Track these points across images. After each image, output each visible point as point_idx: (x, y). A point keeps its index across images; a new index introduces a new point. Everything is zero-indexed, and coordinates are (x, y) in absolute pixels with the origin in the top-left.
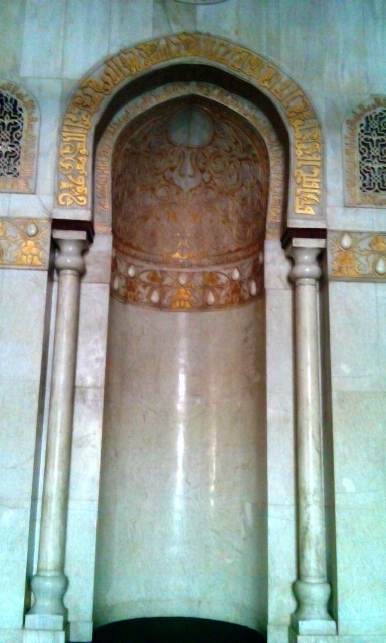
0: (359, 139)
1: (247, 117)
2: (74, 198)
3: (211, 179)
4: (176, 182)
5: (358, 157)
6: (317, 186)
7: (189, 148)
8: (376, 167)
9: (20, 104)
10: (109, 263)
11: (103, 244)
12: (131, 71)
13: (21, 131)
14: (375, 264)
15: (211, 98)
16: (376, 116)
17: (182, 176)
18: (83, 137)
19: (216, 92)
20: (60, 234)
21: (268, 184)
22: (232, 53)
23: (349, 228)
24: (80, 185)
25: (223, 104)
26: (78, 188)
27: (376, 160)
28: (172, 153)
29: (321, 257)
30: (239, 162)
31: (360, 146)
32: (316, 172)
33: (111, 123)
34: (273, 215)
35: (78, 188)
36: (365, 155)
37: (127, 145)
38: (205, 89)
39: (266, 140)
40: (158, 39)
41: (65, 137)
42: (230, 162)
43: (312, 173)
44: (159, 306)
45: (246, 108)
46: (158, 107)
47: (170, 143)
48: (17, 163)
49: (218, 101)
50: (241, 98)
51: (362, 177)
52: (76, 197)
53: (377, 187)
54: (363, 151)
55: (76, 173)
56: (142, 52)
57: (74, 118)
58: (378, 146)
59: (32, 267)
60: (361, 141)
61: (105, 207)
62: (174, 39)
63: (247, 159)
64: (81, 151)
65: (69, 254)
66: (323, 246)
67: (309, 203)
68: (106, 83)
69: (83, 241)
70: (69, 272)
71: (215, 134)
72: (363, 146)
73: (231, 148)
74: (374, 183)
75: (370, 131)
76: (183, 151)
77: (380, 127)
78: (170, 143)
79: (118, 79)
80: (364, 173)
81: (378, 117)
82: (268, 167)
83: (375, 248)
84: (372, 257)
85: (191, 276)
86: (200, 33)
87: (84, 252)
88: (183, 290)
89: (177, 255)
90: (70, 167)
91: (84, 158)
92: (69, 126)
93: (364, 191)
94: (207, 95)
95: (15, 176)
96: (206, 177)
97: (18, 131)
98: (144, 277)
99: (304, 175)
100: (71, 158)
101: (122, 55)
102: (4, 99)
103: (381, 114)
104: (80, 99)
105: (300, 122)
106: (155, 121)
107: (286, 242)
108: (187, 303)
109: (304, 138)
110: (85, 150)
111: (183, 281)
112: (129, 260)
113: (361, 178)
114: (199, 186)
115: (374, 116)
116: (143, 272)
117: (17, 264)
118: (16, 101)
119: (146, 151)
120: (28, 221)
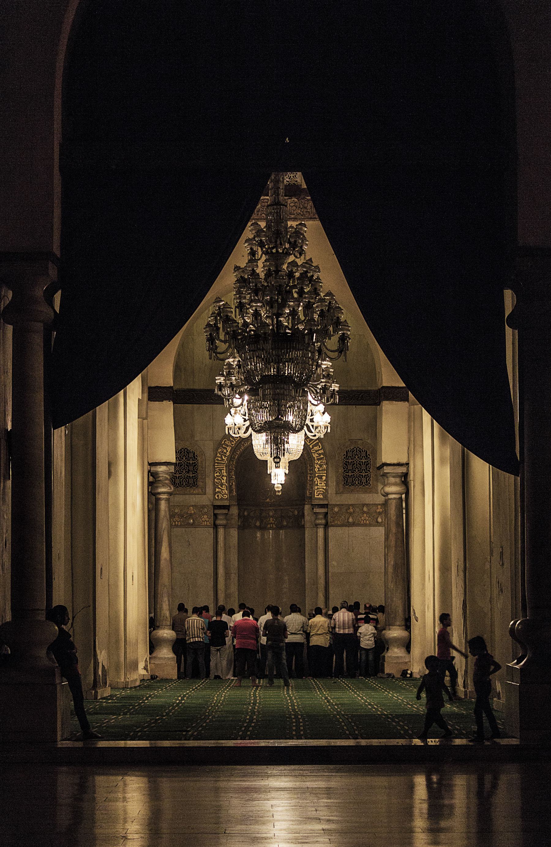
6: (324, 485)
11: (234, 511)
14: (348, 519)
20: (217, 511)
23: (338, 503)
32: (324, 478)
35: (223, 491)
52: (223, 495)
55: (222, 485)
59: (206, 526)
65: (221, 519)
67: (321, 492)
77: (352, 455)
83: (348, 511)
84: (347, 516)
85: (276, 511)
88: (271, 519)
92: (218, 463)
99: (319, 480)
103: (353, 449)
105: (317, 455)
108: (274, 525)
109: (319, 462)
110: (225, 474)
112: (245, 507)
116: (251, 512)
117: (199, 526)
120: (203, 507)
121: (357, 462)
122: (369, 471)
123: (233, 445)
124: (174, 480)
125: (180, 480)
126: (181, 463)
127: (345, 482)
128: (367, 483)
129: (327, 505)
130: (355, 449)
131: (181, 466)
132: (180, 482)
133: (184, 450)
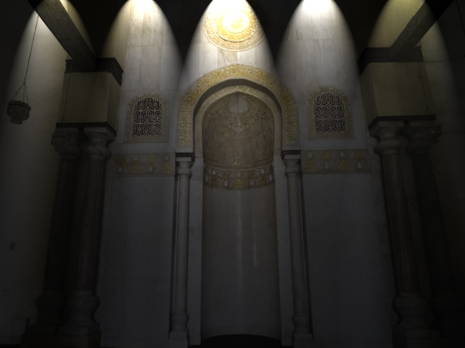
0: (314, 108)
1: (263, 100)
2: (185, 143)
3: (249, 127)
4: (233, 129)
5: (314, 116)
7: (238, 114)
8: (323, 120)
9: (160, 103)
10: (202, 170)
11: (199, 162)
12: (209, 84)
13: (161, 114)
15: (246, 92)
16: (322, 97)
17: (237, 127)
18: (188, 115)
19: (248, 89)
20: (179, 159)
21: (274, 130)
22: (254, 72)
24: (188, 137)
25: (252, 94)
26: (187, 138)
27: (322, 117)
28: (231, 117)
29: (299, 162)
30: (261, 120)
31: (315, 111)
33: (201, 107)
34: (277, 144)
35: (187, 138)
36: (317, 115)
37: (209, 116)
38: (243, 89)
39: (272, 110)
40: (220, 69)
41: (181, 116)
42: (257, 120)
43: (293, 125)
44: (228, 188)
45: (262, 96)
46: (222, 98)
47: (229, 113)
48: (160, 129)
49: (249, 93)
50: (260, 91)
51: (317, 125)
53: (323, 129)
54: (316, 113)
56: (213, 75)
57: (184, 107)
58: (323, 110)
60: (315, 109)
61: (200, 145)
62: (228, 69)
63: (264, 118)
64: (187, 122)
66: (299, 158)
68: (198, 90)
69: (190, 162)
70: (184, 176)
71: (250, 108)
72: (316, 111)
73: (257, 114)
74: (322, 128)
75: (319, 104)
76: (236, 116)
77: (324, 101)
78: (229, 113)
79: (203, 89)
80: (317, 123)
81: (323, 97)
82: (274, 122)
86: (239, 65)
87: (191, 166)
88: (239, 180)
89: (236, 163)
90: (183, 129)
91: (189, 125)
93: (317, 131)
94: (245, 91)
95: (159, 135)
96: (247, 126)
97: (160, 115)
98: (220, 175)
100: (184, 125)
101: (204, 77)
102: (153, 101)
103: (324, 95)
104: (186, 98)
106: (222, 104)
107: (283, 157)
109: (288, 109)
111: (239, 175)
113: (316, 126)
114: (244, 131)
115: (321, 96)
116: (220, 172)
118: (158, 102)
119: (218, 118)
121: (329, 107)
122: (343, 116)
123: (198, 94)
124: (136, 128)
125: (142, 128)
126: (145, 112)
127: (318, 127)
128: (342, 128)
129: (300, 151)
130: (326, 95)
131: (144, 114)
132: (142, 130)
133: (149, 100)
